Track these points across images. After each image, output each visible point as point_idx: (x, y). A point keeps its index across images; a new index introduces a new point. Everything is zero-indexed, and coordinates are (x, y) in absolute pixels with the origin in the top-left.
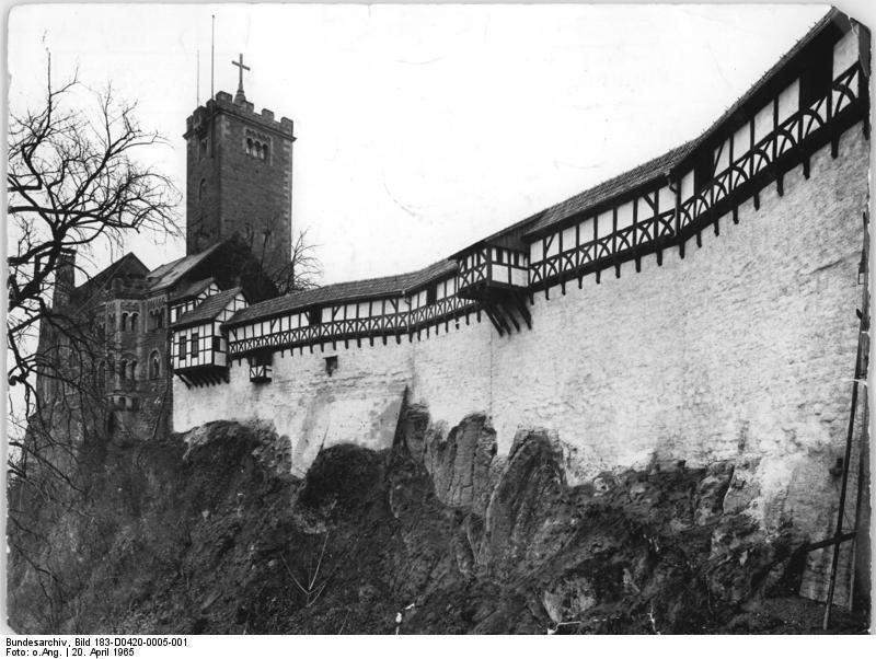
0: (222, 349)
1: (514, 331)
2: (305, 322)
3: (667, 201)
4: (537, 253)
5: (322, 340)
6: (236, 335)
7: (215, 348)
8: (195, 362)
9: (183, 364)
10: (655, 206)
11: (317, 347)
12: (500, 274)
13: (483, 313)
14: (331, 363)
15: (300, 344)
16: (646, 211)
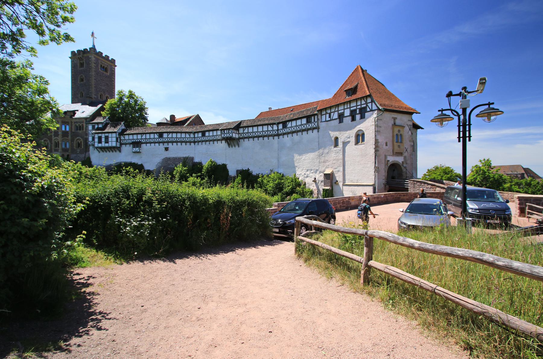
0: (119, 141)
1: (234, 147)
2: (156, 136)
3: (275, 127)
4: (241, 130)
5: (163, 143)
7: (117, 141)
8: (107, 145)
9: (100, 145)
10: (273, 128)
11: (161, 144)
12: (234, 135)
13: (224, 142)
14: (167, 149)
15: (155, 143)
16: (270, 128)
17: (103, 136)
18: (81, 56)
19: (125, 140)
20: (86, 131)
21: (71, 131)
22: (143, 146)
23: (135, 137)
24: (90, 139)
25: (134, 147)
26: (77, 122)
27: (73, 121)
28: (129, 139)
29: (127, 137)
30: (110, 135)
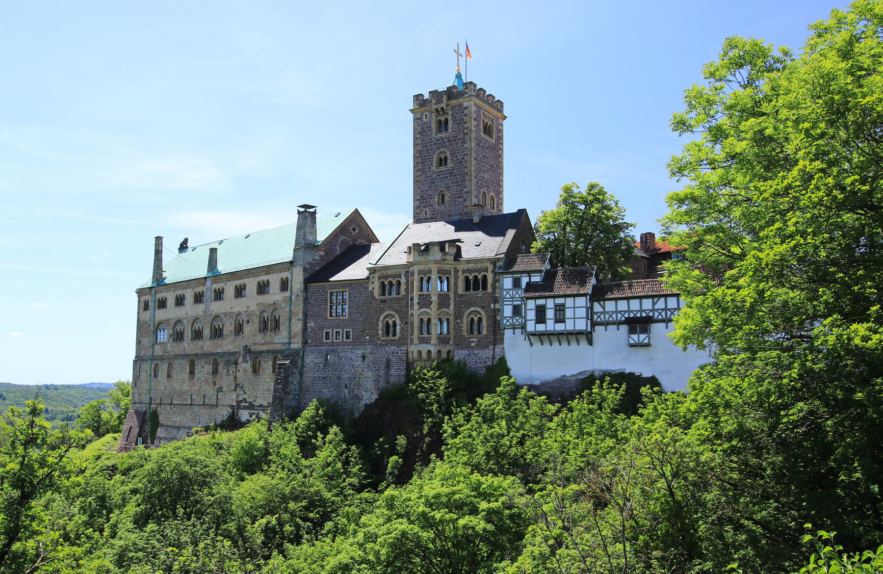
6: (603, 307)
8: (560, 327)
9: (541, 327)
17: (550, 303)
18: (443, 105)
19: (604, 313)
20: (494, 292)
21: (456, 293)
22: (656, 328)
23: (635, 305)
24: (508, 311)
25: (632, 331)
26: (470, 271)
27: (461, 267)
28: (617, 312)
29: (610, 306)
30: (569, 302)
